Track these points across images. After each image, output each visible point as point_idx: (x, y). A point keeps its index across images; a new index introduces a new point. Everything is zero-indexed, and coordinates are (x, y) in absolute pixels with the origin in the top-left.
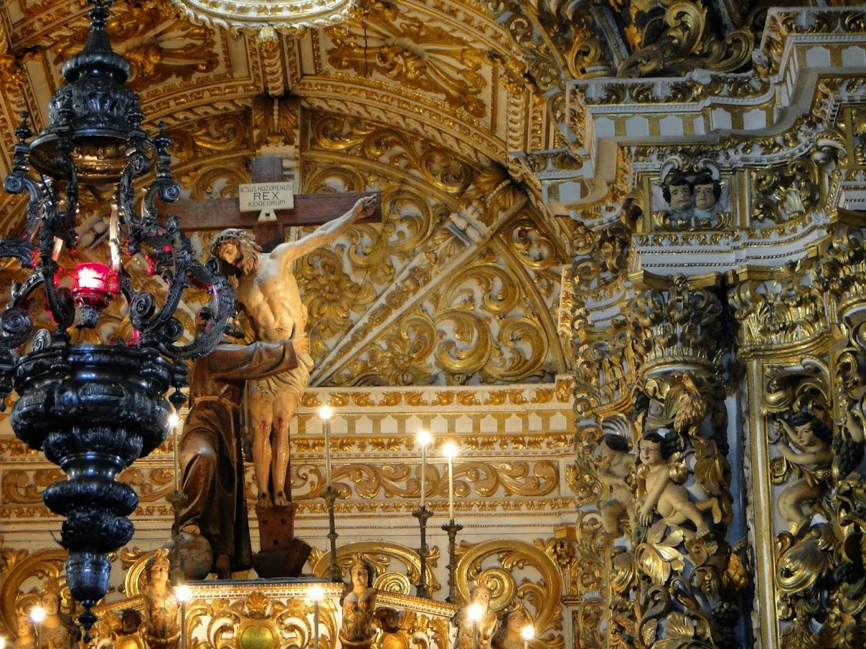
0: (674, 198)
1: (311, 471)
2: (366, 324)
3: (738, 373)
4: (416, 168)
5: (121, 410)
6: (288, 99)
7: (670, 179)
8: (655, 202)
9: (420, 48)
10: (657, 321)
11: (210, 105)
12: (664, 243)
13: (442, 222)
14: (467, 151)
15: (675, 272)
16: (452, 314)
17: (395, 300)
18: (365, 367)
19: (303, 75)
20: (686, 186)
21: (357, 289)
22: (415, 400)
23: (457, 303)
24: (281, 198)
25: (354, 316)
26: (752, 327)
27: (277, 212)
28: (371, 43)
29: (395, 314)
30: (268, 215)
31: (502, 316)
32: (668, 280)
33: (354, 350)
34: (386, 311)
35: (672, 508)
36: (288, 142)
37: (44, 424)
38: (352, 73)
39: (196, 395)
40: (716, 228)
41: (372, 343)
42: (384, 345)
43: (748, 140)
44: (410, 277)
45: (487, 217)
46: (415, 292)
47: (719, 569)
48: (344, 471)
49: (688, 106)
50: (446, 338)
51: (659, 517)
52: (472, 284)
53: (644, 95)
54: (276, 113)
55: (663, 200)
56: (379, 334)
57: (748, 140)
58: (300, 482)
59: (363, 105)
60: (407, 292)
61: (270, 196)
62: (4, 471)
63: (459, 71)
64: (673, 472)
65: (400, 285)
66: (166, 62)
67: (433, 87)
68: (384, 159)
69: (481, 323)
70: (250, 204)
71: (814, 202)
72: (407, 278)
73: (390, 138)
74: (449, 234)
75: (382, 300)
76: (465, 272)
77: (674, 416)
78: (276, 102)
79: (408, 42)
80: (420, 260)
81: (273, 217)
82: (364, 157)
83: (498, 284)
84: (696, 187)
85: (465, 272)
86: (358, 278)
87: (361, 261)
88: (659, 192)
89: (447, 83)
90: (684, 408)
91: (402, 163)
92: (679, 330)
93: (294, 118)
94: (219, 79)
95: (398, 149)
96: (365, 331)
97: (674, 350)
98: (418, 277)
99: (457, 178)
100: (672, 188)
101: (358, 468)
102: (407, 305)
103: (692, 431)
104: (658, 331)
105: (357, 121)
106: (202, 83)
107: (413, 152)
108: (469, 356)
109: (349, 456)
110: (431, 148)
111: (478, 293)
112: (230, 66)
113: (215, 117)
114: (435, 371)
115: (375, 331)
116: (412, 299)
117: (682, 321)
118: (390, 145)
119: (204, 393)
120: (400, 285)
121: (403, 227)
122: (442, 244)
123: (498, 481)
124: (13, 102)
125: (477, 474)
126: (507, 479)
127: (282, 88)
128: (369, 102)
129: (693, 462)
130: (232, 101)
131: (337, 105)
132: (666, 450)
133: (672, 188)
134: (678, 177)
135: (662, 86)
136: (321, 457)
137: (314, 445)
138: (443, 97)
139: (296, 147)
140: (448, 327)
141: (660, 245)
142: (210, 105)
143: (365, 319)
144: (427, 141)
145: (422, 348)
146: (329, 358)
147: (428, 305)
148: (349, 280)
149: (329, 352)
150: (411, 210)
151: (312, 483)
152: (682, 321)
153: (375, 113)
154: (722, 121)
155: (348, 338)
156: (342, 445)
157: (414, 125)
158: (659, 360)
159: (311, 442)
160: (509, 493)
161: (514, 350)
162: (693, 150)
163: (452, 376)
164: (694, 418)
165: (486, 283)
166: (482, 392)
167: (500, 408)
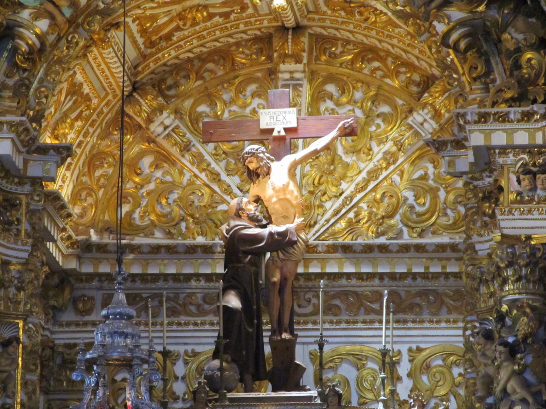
0: (523, 183)
2: (352, 192)
6: (298, 29)
7: (521, 170)
10: (510, 264)
11: (244, 32)
12: (516, 213)
13: (406, 118)
15: (523, 233)
17: (373, 174)
20: (531, 175)
24: (288, 120)
27: (286, 130)
30: (279, 132)
32: (517, 238)
35: (515, 391)
36: (298, 61)
49: (531, 125)
51: (509, 395)
53: (504, 118)
54: (290, 40)
55: (516, 183)
61: (281, 118)
62: (103, 294)
64: (516, 367)
70: (267, 124)
72: (381, 159)
73: (370, 56)
77: (518, 330)
78: (290, 33)
81: (283, 133)
84: (538, 176)
86: (347, 159)
88: (514, 178)
91: (379, 73)
92: (524, 272)
95: (376, 64)
97: (520, 284)
100: (522, 177)
101: (346, 294)
103: (529, 341)
104: (510, 272)
107: (386, 66)
116: (385, 174)
117: (526, 266)
118: (369, 61)
120: (376, 163)
121: (379, 121)
129: (529, 359)
130: (259, 29)
131: (333, 31)
133: (522, 177)
135: (515, 112)
141: (513, 215)
142: (244, 32)
143: (352, 188)
144: (397, 58)
152: (526, 266)
164: (530, 333)
167: (444, 255)
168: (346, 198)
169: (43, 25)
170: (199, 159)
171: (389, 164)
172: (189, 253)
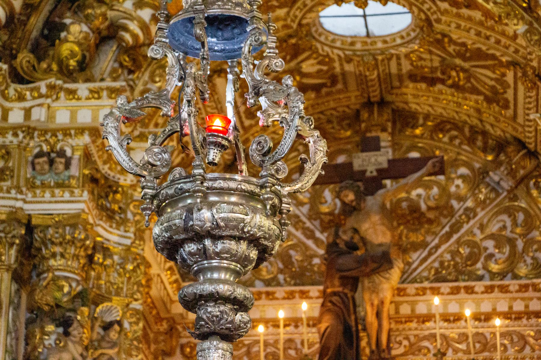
1: (404, 338)
2: (436, 244)
4: (465, 144)
5: (244, 226)
6: (382, 103)
9: (466, 65)
13: (484, 177)
14: (499, 133)
16: (492, 236)
18: (437, 272)
19: (392, 88)
21: (430, 222)
22: (470, 290)
25: (429, 239)
28: (436, 64)
29: (455, 237)
30: (371, 172)
31: (523, 236)
33: (429, 261)
34: (449, 236)
37: (183, 236)
38: (424, 86)
39: (327, 288)
41: (441, 256)
42: (448, 257)
44: (464, 213)
45: (512, 173)
46: (468, 222)
48: (425, 338)
50: (488, 252)
52: (505, 217)
56: (445, 250)
58: (396, 346)
59: (431, 106)
60: (464, 223)
63: (492, 79)
65: (458, 218)
66: (306, 81)
67: (475, 91)
68: (446, 139)
69: (511, 242)
74: (488, 185)
75: (447, 229)
79: (458, 61)
80: (470, 203)
81: (375, 174)
82: (432, 139)
83: (521, 217)
86: (431, 215)
87: (432, 203)
89: (485, 88)
91: (457, 142)
93: (387, 114)
94: (339, 92)
95: (454, 133)
96: (437, 247)
98: (470, 213)
99: (493, 150)
102: (463, 231)
105: (427, 117)
106: (328, 94)
108: (504, 262)
109: (428, 329)
111: (509, 224)
112: (345, 83)
113: (337, 117)
114: (480, 273)
115: (443, 247)
116: (466, 227)
118: (448, 131)
119: (333, 286)
120: (458, 218)
121: (459, 182)
123: (526, 343)
124: (209, 106)
125: (512, 338)
126: (531, 341)
127: (379, 96)
128: (435, 104)
130: (348, 107)
136: (410, 329)
137: (406, 322)
138: (481, 98)
139: (389, 134)
140: (490, 244)
142: (334, 109)
143: (436, 241)
144: (472, 127)
145: (473, 258)
146: (414, 266)
147: (477, 231)
148: (425, 217)
149: (414, 262)
150: (463, 170)
151: (405, 346)
153: (440, 110)
155: (426, 253)
156: (423, 322)
157: (465, 118)
159: (403, 320)
160: (533, 350)
161: (533, 258)
163: (493, 275)
167: (526, 295)
168: (431, 249)
171: (469, 219)
172: (288, 298)
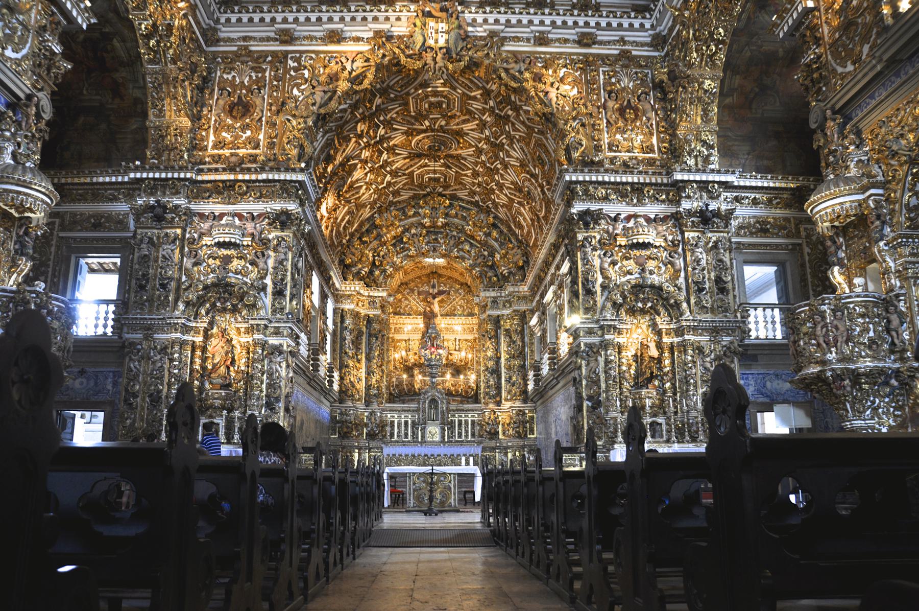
3: (500, 328)
6: (436, 272)
8: (489, 304)
23: (460, 303)
26: (502, 323)
40: (498, 308)
43: (502, 297)
47: (496, 354)
53: (489, 291)
57: (502, 297)
71: (511, 306)
76: (461, 299)
85: (461, 299)
90: (493, 333)
98: (454, 300)
110: (456, 280)
122: (458, 295)
132: (490, 339)
134: (493, 301)
135: (491, 289)
145: (454, 310)
154: (499, 294)
158: (489, 327)
162: (494, 298)
165: (464, 300)
166: (463, 318)
169: (391, 269)
170: (414, 299)
